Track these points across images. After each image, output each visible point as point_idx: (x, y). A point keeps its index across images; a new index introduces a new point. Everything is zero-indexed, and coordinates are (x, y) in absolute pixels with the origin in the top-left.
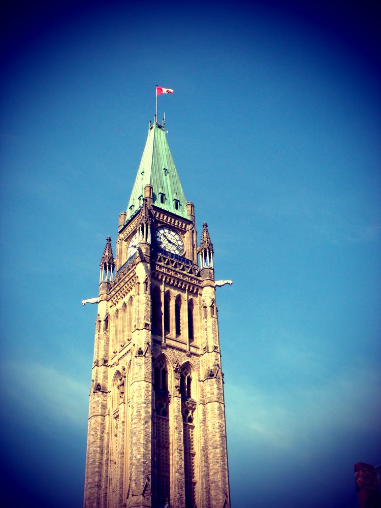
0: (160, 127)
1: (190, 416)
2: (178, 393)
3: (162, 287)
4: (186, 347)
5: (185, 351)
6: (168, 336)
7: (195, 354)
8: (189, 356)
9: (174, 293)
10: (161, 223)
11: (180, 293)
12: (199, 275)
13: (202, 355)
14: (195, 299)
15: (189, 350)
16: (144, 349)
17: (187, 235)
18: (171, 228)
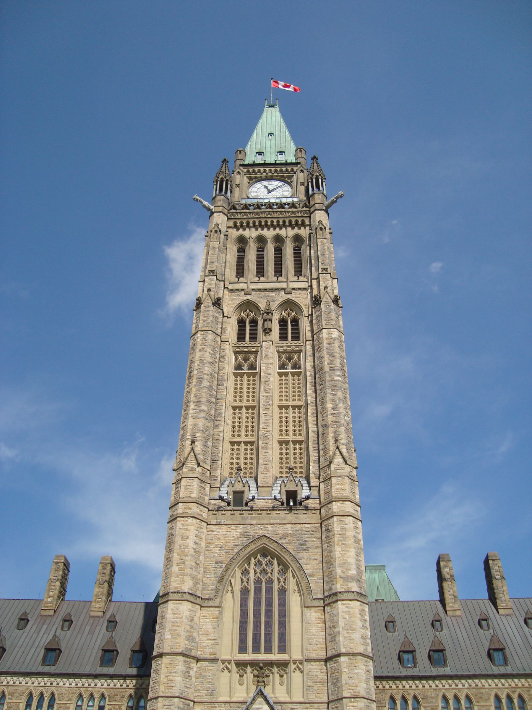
4: (284, 285)
5: (283, 289)
10: (256, 178)
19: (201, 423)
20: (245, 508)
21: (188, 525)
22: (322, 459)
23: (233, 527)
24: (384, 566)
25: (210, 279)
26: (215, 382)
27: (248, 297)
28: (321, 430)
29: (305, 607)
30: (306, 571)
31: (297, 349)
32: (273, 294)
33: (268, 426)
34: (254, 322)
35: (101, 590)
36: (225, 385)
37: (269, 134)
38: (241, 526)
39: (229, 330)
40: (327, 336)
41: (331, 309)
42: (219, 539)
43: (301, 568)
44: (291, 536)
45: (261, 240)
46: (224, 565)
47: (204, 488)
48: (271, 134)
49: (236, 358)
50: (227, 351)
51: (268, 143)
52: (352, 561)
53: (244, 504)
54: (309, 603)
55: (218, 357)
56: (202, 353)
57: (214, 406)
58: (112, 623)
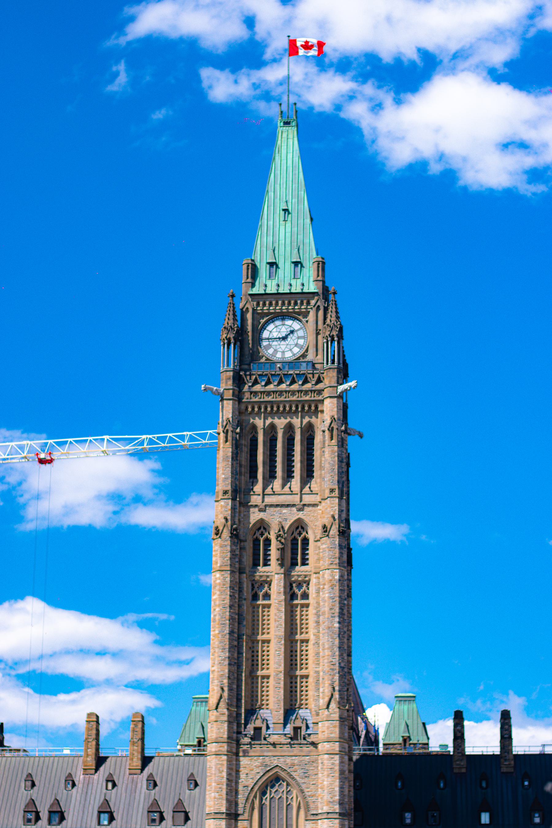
0: (287, 123)
1: (305, 591)
2: (279, 567)
3: (259, 422)
5: (294, 505)
6: (269, 490)
7: (309, 505)
8: (299, 510)
9: (281, 423)
11: (289, 420)
12: (319, 381)
13: (320, 502)
14: (313, 420)
15: (301, 501)
16: (221, 528)
17: (311, 316)
18: (283, 316)
19: (227, 671)
20: (263, 742)
21: (223, 761)
22: (321, 701)
23: (255, 758)
24: (414, 697)
25: (225, 502)
26: (236, 624)
27: (262, 515)
28: (321, 674)
29: (306, 820)
30: (307, 794)
31: (307, 579)
32: (284, 511)
33: (280, 665)
34: (268, 542)
35: (135, 748)
36: (245, 623)
37: (283, 210)
38: (261, 758)
39: (245, 557)
40: (331, 578)
41: (335, 544)
42: (245, 767)
43: (302, 791)
44: (297, 765)
45: (273, 427)
46: (250, 788)
47: (232, 728)
48: (286, 210)
49: (253, 585)
50: (245, 586)
51: (282, 228)
52: (337, 789)
53: (262, 739)
54: (309, 818)
55: (237, 596)
56: (223, 597)
57: (236, 649)
58: (153, 783)
